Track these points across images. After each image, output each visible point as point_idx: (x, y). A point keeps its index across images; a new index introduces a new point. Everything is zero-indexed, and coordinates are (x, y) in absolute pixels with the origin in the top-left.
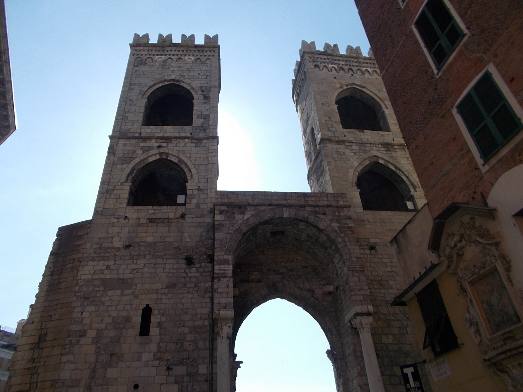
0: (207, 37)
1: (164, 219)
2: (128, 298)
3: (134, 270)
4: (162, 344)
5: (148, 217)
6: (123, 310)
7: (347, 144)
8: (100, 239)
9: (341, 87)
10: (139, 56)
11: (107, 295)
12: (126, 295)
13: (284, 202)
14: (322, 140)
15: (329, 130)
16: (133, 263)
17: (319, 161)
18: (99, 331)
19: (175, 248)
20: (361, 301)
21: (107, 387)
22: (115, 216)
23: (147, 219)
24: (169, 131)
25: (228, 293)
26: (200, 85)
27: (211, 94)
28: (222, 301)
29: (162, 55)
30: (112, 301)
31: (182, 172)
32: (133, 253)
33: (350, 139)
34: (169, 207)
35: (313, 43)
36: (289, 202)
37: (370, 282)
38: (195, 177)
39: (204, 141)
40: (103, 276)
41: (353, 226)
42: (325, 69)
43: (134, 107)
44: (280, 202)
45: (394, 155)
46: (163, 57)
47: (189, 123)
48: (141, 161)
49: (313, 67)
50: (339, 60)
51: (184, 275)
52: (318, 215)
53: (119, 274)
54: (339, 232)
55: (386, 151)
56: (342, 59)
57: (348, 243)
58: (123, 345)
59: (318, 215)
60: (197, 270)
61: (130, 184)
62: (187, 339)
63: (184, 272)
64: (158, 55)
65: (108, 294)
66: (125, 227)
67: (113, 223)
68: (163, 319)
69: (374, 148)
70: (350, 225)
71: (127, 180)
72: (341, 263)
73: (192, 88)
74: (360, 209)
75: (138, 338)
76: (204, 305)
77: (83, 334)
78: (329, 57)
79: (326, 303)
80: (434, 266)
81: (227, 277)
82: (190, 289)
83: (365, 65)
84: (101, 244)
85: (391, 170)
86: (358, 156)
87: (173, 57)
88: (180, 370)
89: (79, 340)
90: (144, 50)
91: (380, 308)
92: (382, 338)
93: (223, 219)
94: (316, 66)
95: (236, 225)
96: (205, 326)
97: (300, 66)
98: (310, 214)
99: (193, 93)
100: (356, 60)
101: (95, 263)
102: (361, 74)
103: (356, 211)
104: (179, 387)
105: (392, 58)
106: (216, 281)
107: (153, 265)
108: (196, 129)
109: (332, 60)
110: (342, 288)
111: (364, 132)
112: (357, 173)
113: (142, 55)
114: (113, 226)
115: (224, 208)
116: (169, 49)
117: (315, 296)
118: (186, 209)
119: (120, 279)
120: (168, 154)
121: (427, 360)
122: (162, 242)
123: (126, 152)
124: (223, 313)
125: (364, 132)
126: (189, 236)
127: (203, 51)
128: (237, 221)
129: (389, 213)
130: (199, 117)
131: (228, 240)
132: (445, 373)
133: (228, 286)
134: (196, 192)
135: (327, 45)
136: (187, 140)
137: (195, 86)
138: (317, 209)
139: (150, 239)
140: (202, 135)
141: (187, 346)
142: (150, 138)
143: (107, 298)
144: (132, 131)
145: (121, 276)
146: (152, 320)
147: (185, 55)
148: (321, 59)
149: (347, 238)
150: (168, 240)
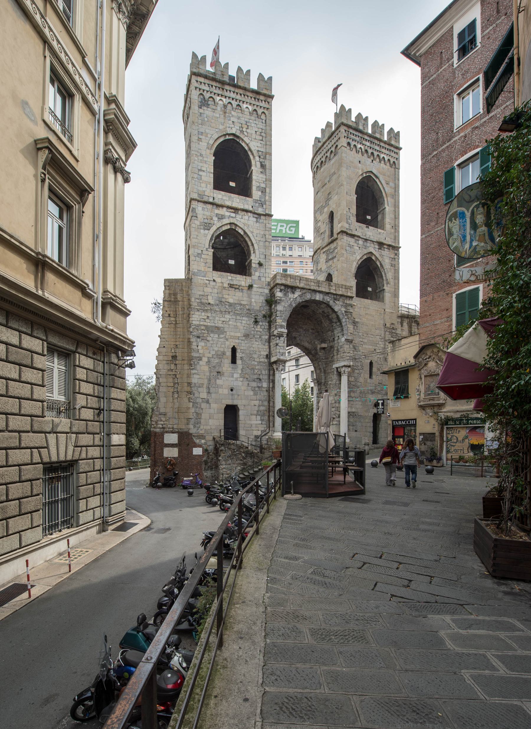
1: (239, 286)
8: (200, 295)
18: (208, 358)
26: (257, 149)
27: (267, 163)
29: (222, 96)
38: (257, 252)
39: (262, 217)
40: (205, 324)
43: (205, 165)
46: (224, 99)
64: (218, 95)
75: (231, 365)
76: (265, 350)
77: (200, 359)
84: (201, 299)
87: (234, 102)
88: (254, 384)
101: (200, 313)
113: (204, 90)
114: (206, 287)
116: (227, 87)
119: (216, 327)
120: (236, 225)
128: (290, 299)
134: (257, 266)
136: (249, 214)
137: (253, 149)
138: (335, 297)
139: (231, 301)
140: (260, 211)
142: (222, 206)
145: (217, 325)
147: (243, 102)
150: (243, 302)
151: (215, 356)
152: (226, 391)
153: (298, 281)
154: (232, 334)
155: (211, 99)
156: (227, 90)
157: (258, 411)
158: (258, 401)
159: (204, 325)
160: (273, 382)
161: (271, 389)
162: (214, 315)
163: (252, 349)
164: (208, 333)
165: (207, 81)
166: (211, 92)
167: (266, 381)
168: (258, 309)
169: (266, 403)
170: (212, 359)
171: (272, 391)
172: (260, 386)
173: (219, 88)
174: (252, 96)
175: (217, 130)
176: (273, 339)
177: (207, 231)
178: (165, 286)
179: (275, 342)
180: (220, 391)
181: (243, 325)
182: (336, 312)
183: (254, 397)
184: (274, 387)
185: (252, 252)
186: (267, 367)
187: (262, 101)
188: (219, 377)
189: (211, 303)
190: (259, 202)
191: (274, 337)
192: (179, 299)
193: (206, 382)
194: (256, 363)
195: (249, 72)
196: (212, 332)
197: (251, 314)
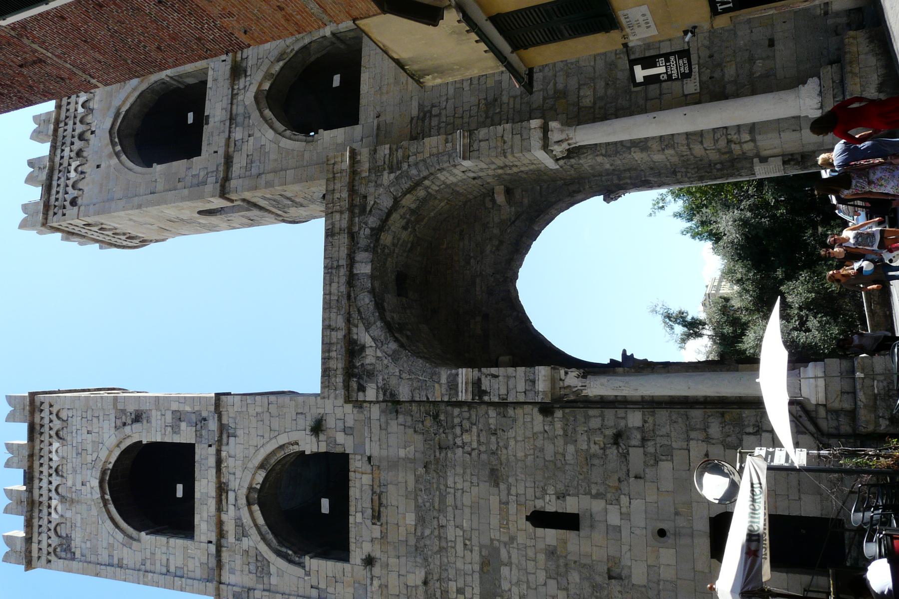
0: (11, 418)
1: (373, 493)
3: (465, 545)
4: (594, 492)
5: (369, 522)
6: (535, 560)
7: (231, 149)
9: (117, 155)
10: (51, 550)
11: (510, 590)
12: (510, 557)
13: (343, 271)
14: (223, 194)
15: (205, 183)
16: (454, 547)
17: (262, 203)
19: (426, 471)
20: (522, 140)
21: (661, 583)
22: (368, 584)
23: (373, 524)
24: (205, 487)
25: (508, 377)
26: (113, 430)
27: (131, 408)
28: (521, 387)
29: (49, 506)
30: (519, 581)
31: (284, 462)
32: (436, 548)
33: (222, 143)
34: (351, 484)
35: (25, 208)
36: (343, 262)
37: (489, 120)
39: (224, 421)
41: (388, 146)
42: (80, 185)
43: (158, 556)
44: (343, 280)
45: (255, 61)
46: (54, 503)
47: (188, 450)
48: (264, 539)
49: (76, 209)
50: (62, 157)
51: (474, 454)
52: (368, 209)
53: (473, 572)
54: (398, 172)
55: (246, 76)
56: (59, 151)
57: (420, 157)
58: (594, 558)
59: (368, 209)
60: (467, 431)
61: (307, 558)
62: (585, 447)
63: (470, 454)
64: (50, 514)
65: (507, 589)
66: (388, 565)
67: (380, 586)
68: (551, 490)
69: (240, 98)
70: (387, 152)
71: (301, 565)
72: (455, 171)
73: (118, 446)
74: (357, 130)
75: (582, 533)
78: (55, 177)
79: (526, 201)
80: (467, 18)
81: (479, 380)
82: (501, 444)
83: (72, 107)
85: (282, 68)
86: (256, 130)
88: (636, 456)
90: (39, 542)
91: (534, 106)
92: (586, 107)
93: (374, 386)
94: (73, 202)
95: (386, 362)
96: (564, 416)
97: (69, 234)
98: (366, 224)
99: (128, 442)
100: (62, 125)
102: (90, 117)
103: (360, 138)
104: (663, 461)
105: (68, 66)
106: (486, 398)
109: (60, 171)
110: (500, 171)
111: (208, 116)
112: (288, 133)
113: (49, 545)
114: (387, 586)
115: (354, 385)
116: (36, 493)
117: (513, 219)
118: (355, 454)
119: (482, 569)
120: (250, 489)
121: (624, 41)
122: (416, 496)
123: (246, 568)
124: (542, 385)
125: (208, 116)
127: (42, 426)
128: (378, 358)
129: (365, 77)
130: (175, 429)
131: (413, 377)
132: (644, 15)
133: (496, 377)
134: (322, 437)
135: (30, 180)
136: (224, 454)
138: (357, 211)
139: (411, 519)
140: (213, 425)
141: (597, 447)
142: (220, 524)
143: (515, 590)
144: (204, 559)
145: (477, 567)
146: (553, 510)
147: (51, 460)
148: (58, 192)
149: (412, 159)
152: (667, 555)
154: (495, 521)
158: (692, 444)
162: (452, 573)
163: (530, 458)
168: (420, 437)
169: (697, 414)
170: (572, 592)
172: (639, 437)
175: (100, 522)
177: (273, 569)
181: (467, 484)
182: (396, 201)
183: (679, 456)
185: (296, 448)
186: (580, 413)
189: (423, 574)
190: (199, 426)
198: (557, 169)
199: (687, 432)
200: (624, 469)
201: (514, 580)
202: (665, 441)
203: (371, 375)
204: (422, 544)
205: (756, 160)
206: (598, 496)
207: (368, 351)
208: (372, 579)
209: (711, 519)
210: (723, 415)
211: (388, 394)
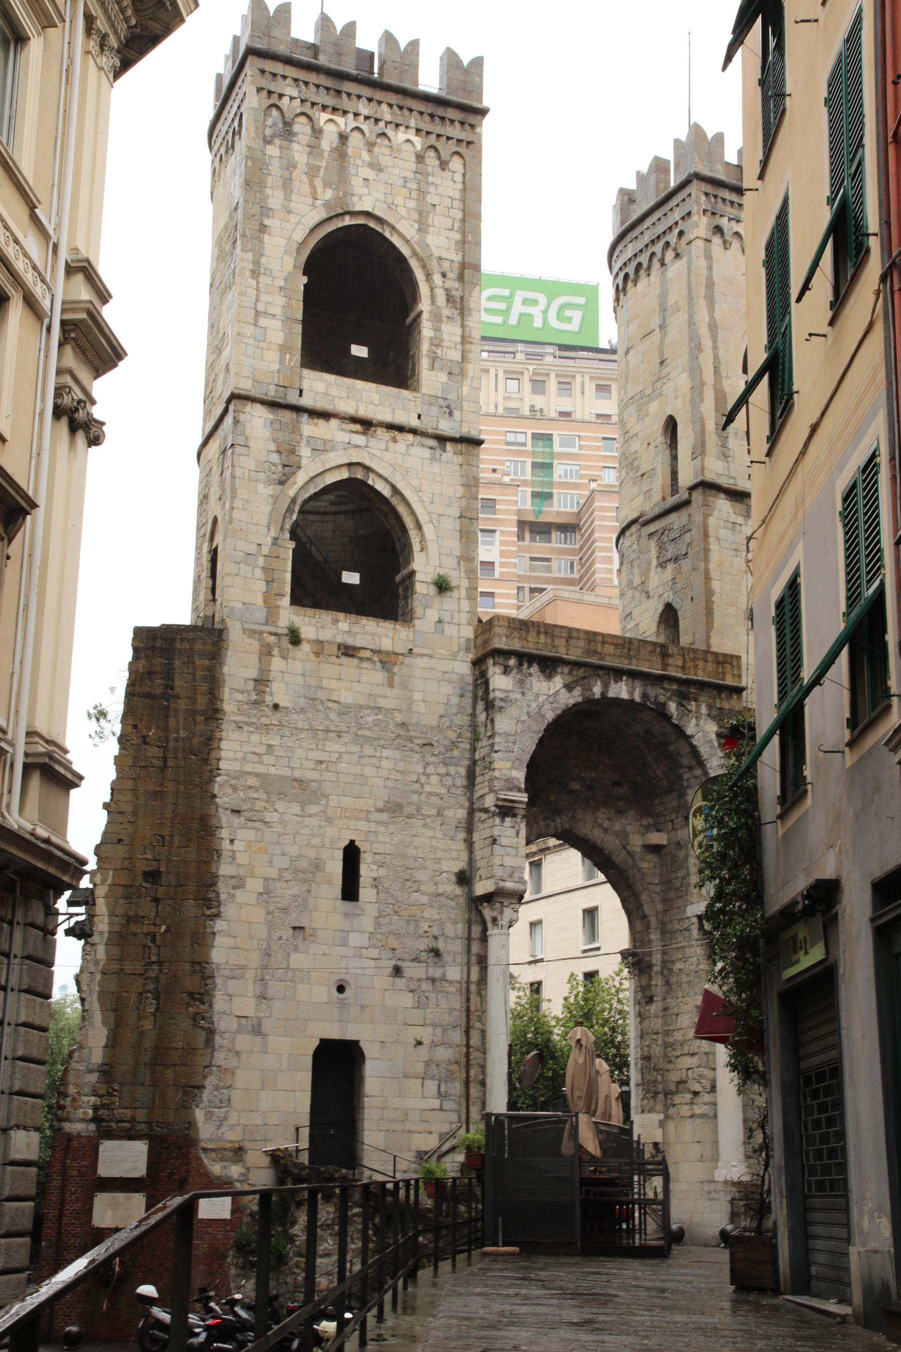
2: (314, 822)
3: (321, 762)
5: (339, 639)
11: (276, 810)
18: (266, 879)
23: (339, 646)
25: (516, 848)
29: (335, 110)
32: (316, 725)
40: (261, 769)
42: (736, 244)
46: (340, 120)
52: (685, 703)
53: (293, 769)
54: (716, 744)
58: (315, 913)
59: (685, 703)
60: (441, 781)
64: (324, 108)
68: (382, 872)
76: (454, 855)
81: (515, 815)
82: (428, 820)
87: (365, 128)
89: (234, 896)
93: (510, 688)
98: (670, 699)
101: (244, 736)
107: (356, 756)
108: (431, 405)
113: (281, 96)
117: (629, 848)
119: (296, 780)
120: (368, 469)
126: (424, 701)
128: (538, 695)
133: (518, 834)
134: (433, 590)
138: (683, 689)
139: (347, 697)
141: (426, 929)
142: (325, 415)
145: (297, 774)
150: (382, 703)
151: (288, 875)
153: (562, 642)
154: (347, 802)
155: (303, 119)
156: (349, 95)
157: (428, 1064)
158: (430, 1030)
159: (257, 775)
160: (483, 961)
161: (473, 988)
162: (289, 742)
164: (267, 802)
165: (292, 72)
166: (302, 101)
167: (459, 958)
168: (434, 723)
169: (457, 1037)
170: (278, 885)
171: (479, 993)
173: (328, 89)
174: (423, 109)
176: (483, 821)
178: (136, 649)
179: (487, 833)
180: (303, 990)
181: (384, 773)
182: (687, 738)
183: (417, 1016)
184: (483, 980)
185: (416, 547)
187: (452, 121)
188: (299, 941)
190: (442, 402)
191: (484, 816)
192: (178, 690)
193: (254, 959)
194: (424, 899)
195: (414, 45)
196: (282, 795)
197: (410, 739)
198: (684, 911)
199: (440, 1025)
200: (405, 957)
201: (286, 818)
202: (432, 1001)
203: (521, 682)
204: (320, 707)
205: (662, 1116)
206: (378, 925)
207: (545, 684)
208: (275, 634)
209: (357, 1042)
210: (456, 1063)
211: (502, 704)
